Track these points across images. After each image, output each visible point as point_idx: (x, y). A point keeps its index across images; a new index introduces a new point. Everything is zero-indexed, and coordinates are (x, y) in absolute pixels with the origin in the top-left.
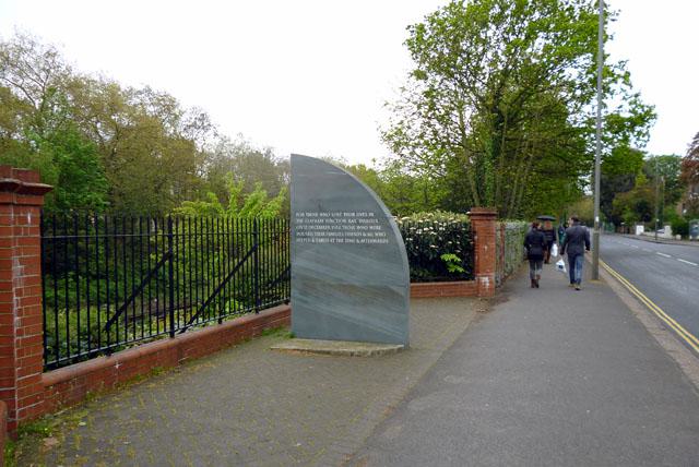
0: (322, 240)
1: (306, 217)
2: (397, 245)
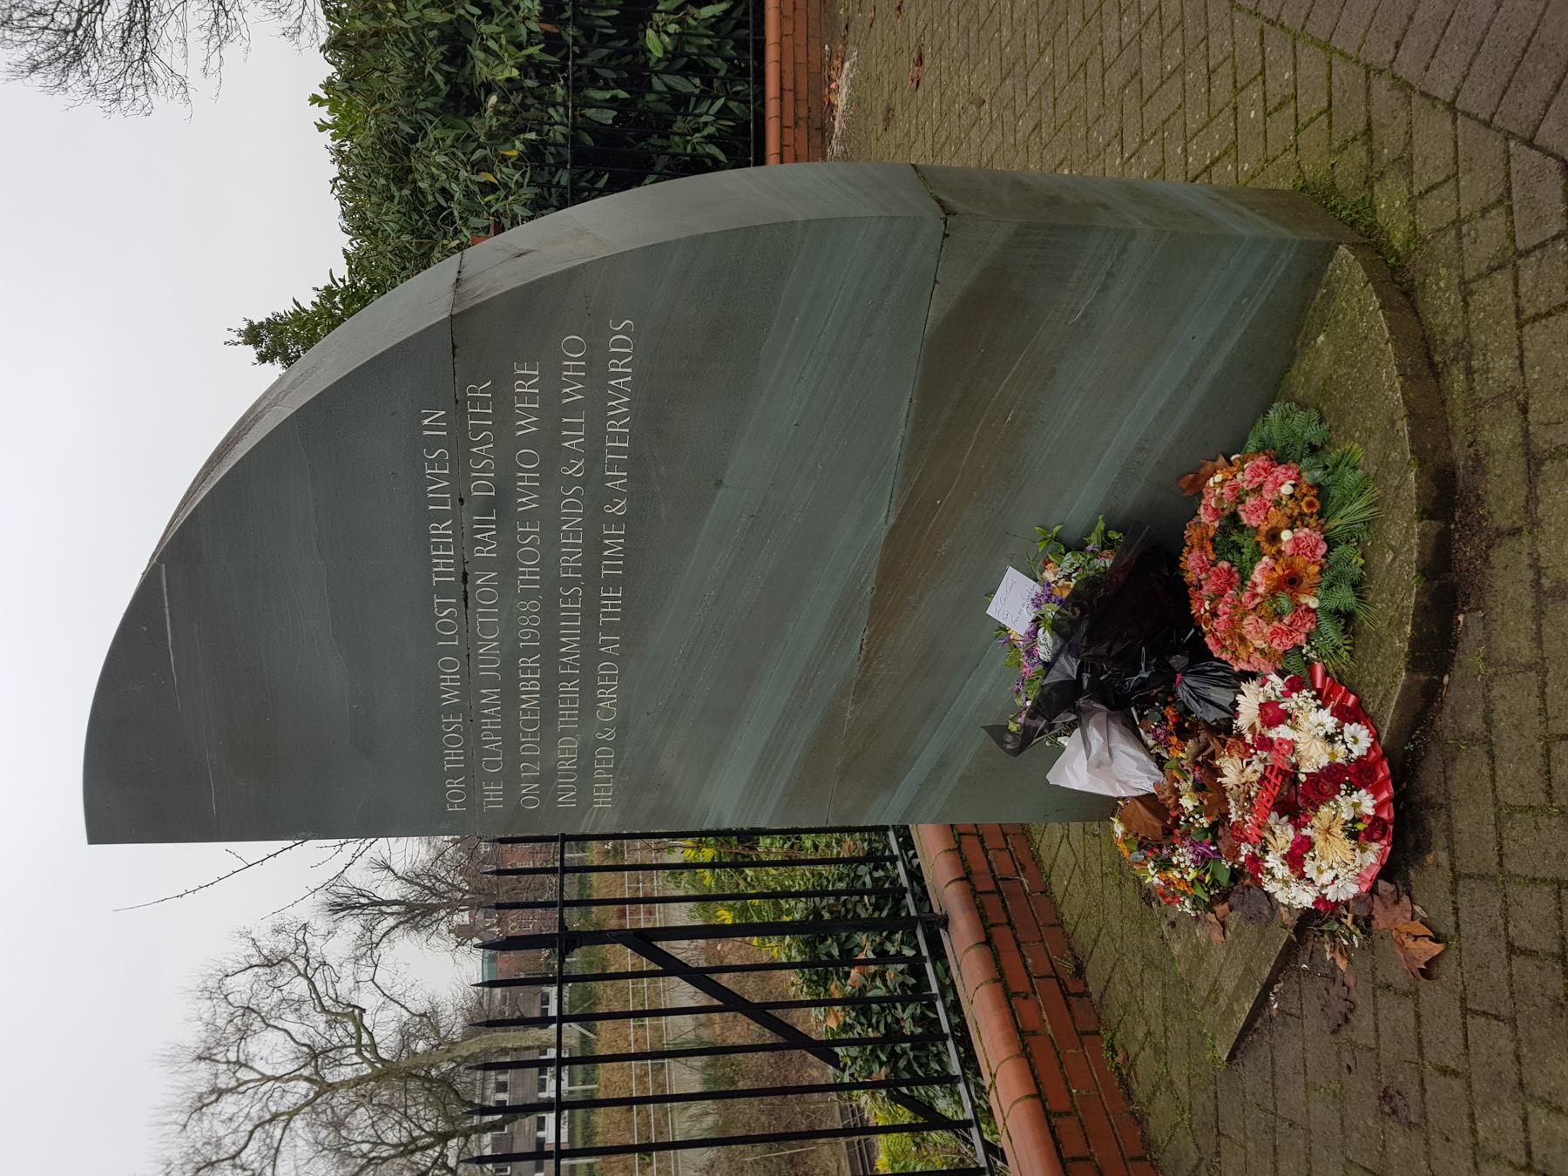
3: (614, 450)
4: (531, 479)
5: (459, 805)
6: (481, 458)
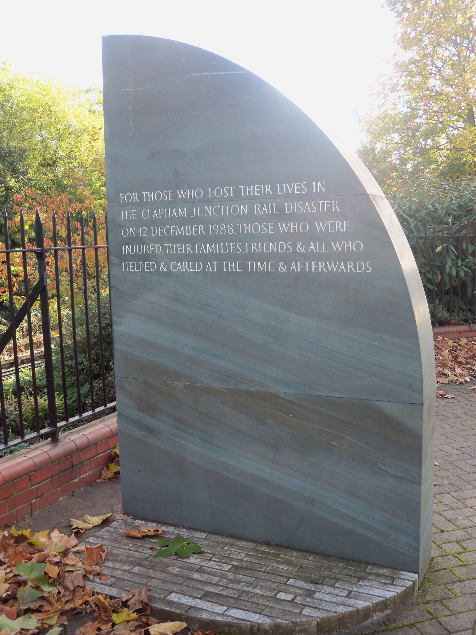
0: (183, 267)
1: (142, 204)
2: (399, 276)
3: (310, 265)
4: (294, 229)
5: (123, 200)
6: (303, 206)
